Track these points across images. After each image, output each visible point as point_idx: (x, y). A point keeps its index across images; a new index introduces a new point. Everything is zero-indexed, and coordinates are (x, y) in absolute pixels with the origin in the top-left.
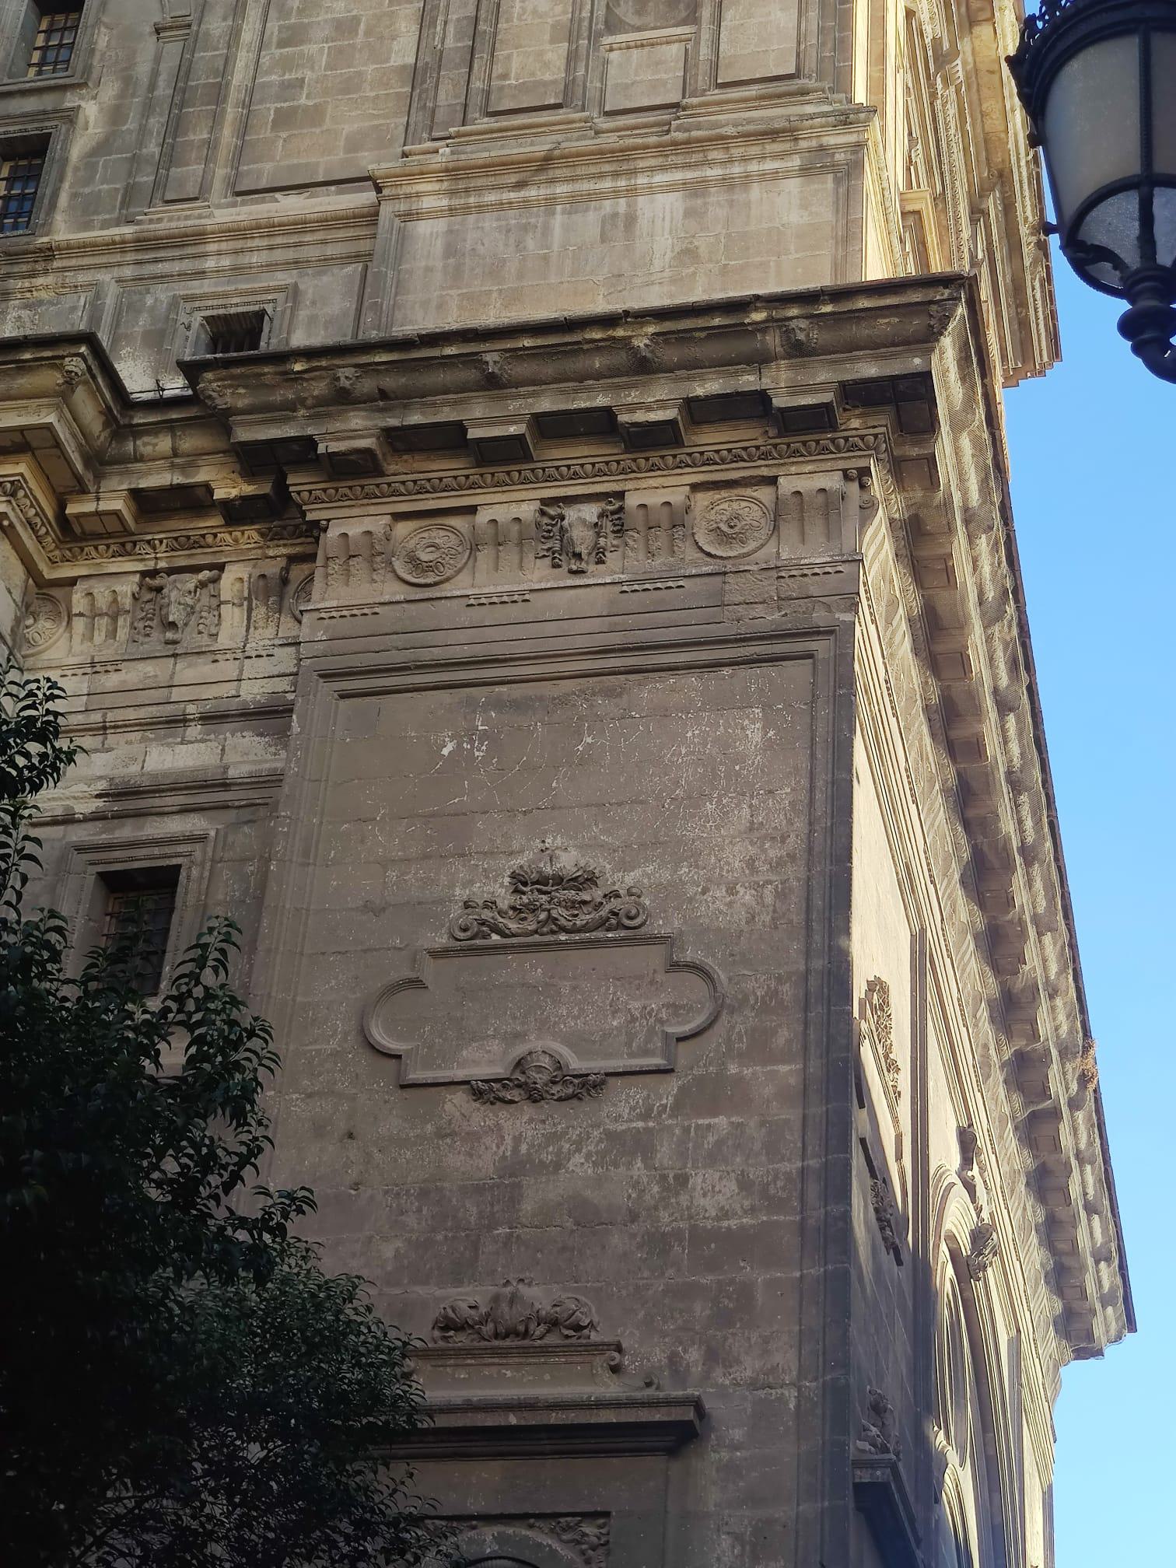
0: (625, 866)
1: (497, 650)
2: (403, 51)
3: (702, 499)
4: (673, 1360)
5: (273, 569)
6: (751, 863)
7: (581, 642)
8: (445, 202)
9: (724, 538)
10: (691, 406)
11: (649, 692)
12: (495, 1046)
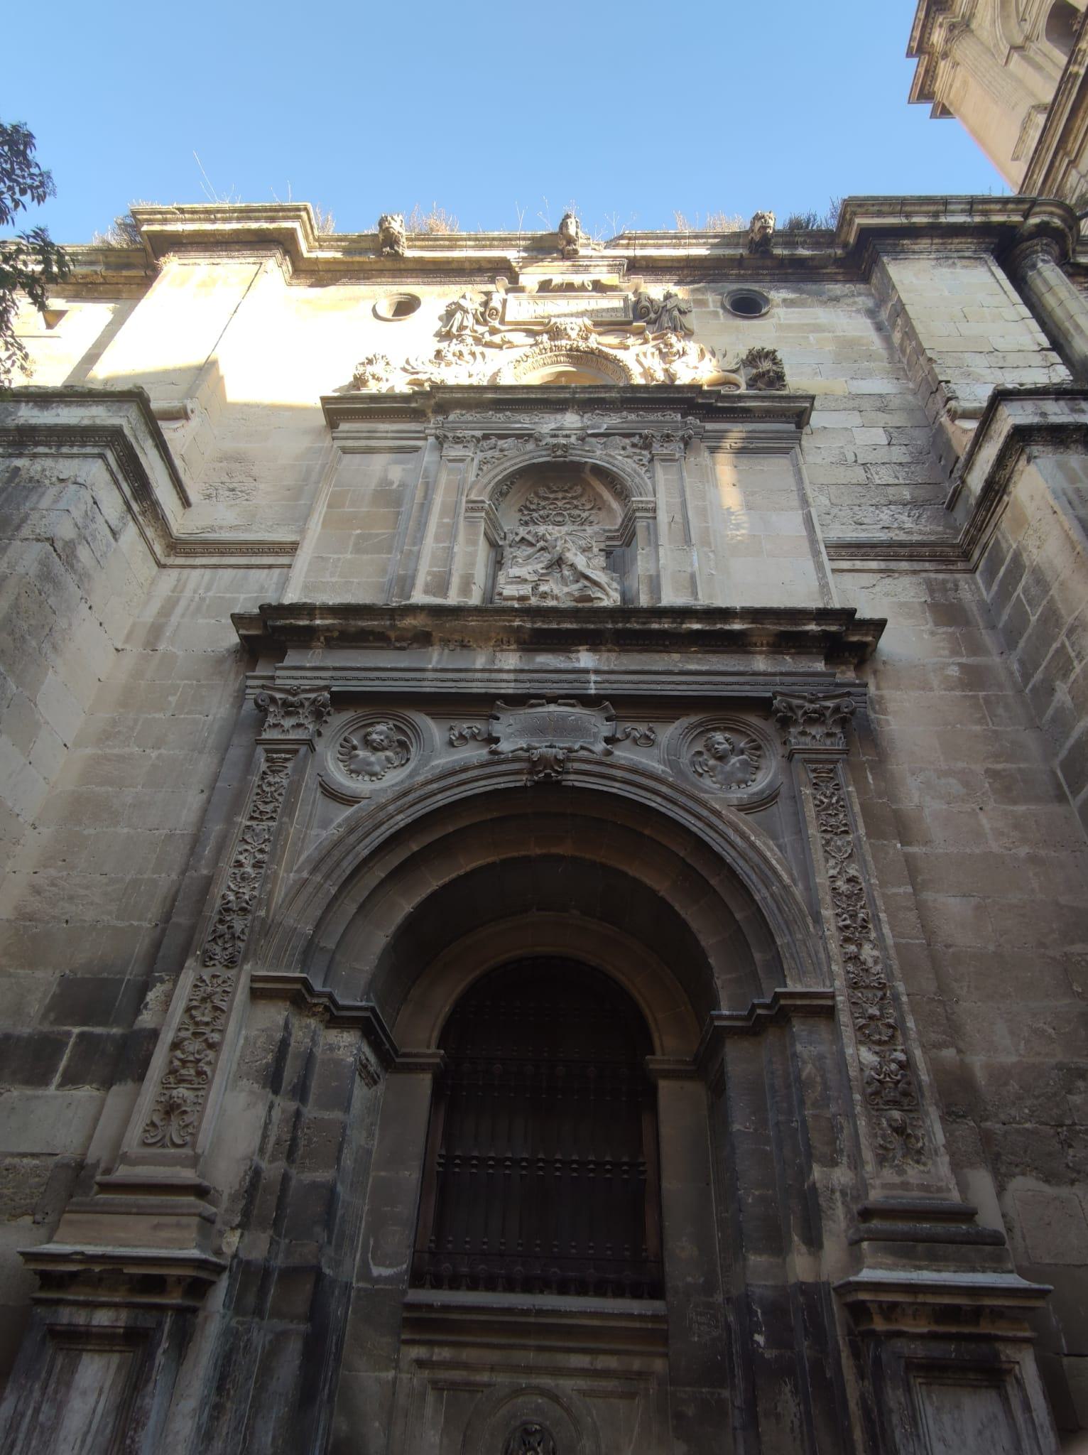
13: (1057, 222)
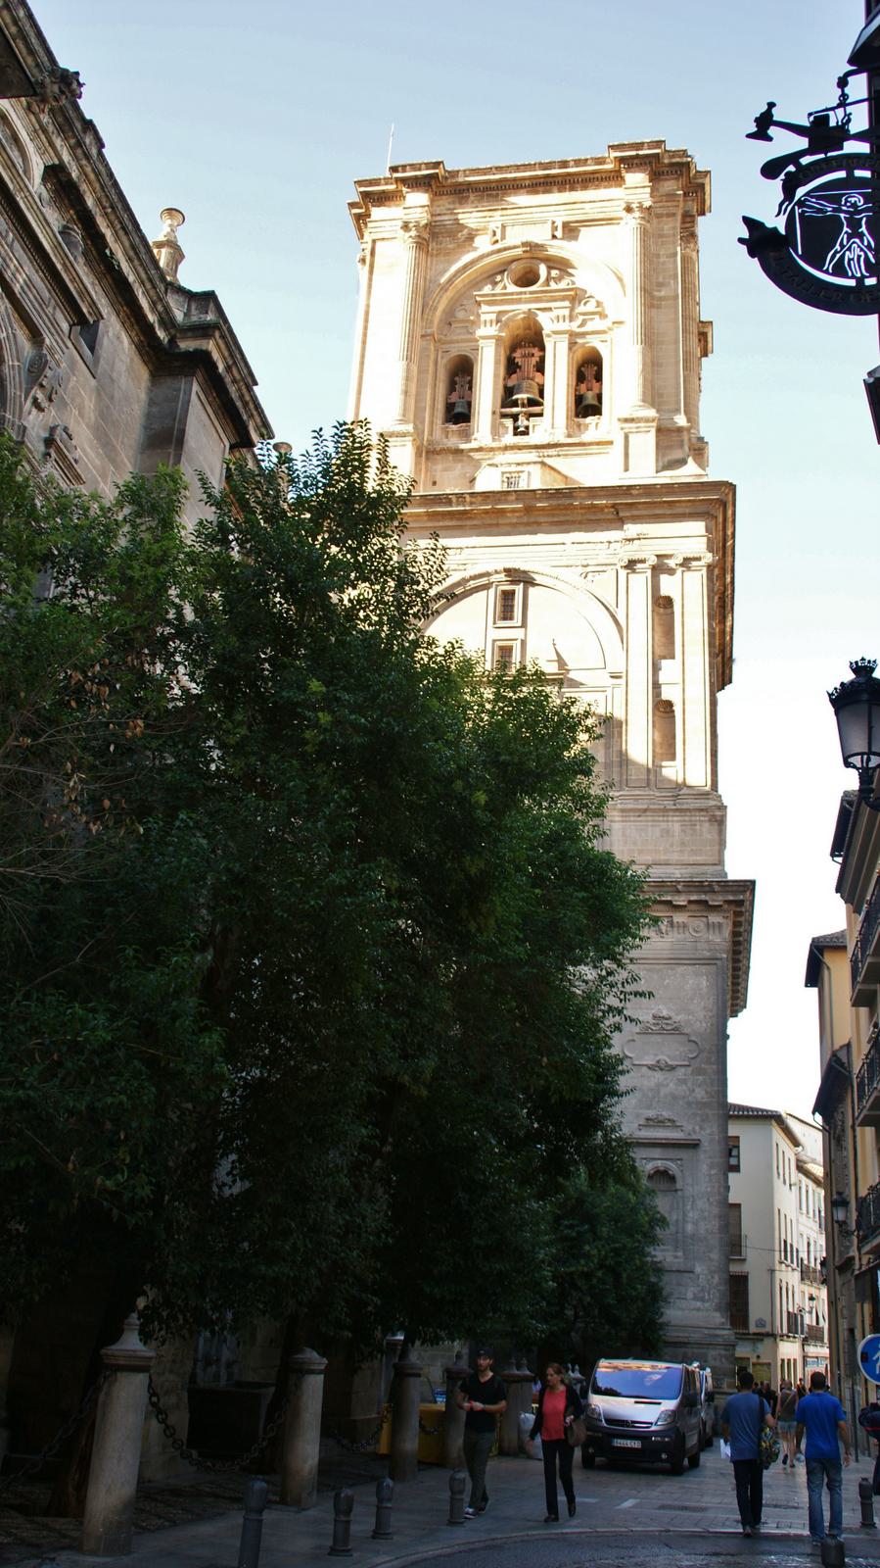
0: (677, 1015)
1: (644, 956)
4: (694, 1128)
6: (705, 1016)
7: (665, 956)
8: (620, 819)
9: (697, 932)
10: (690, 902)
11: (681, 969)
12: (652, 1057)
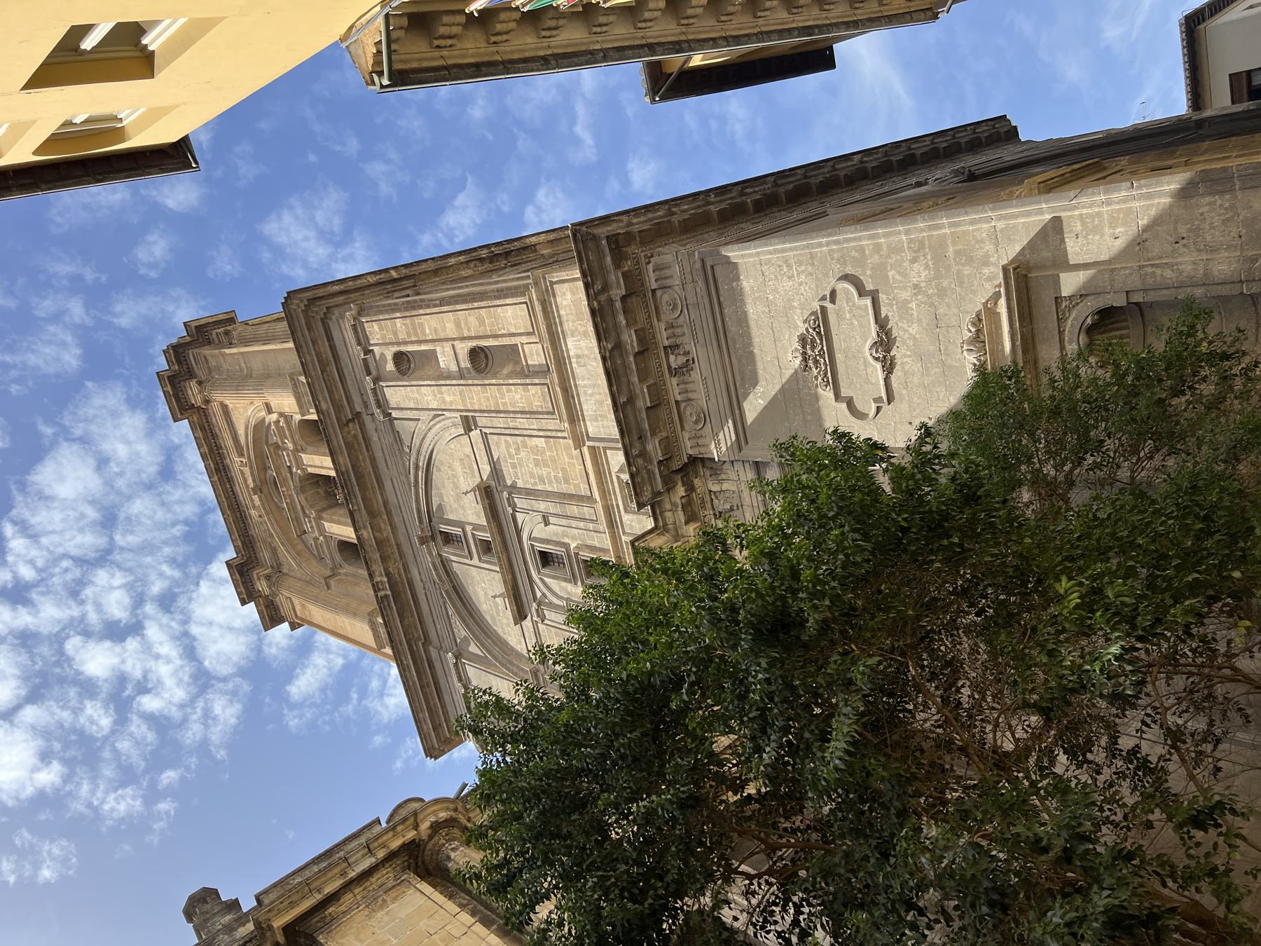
2: (541, 442)
3: (663, 317)
5: (708, 473)
6: (790, 278)
9: (675, 306)
13: (443, 815)
